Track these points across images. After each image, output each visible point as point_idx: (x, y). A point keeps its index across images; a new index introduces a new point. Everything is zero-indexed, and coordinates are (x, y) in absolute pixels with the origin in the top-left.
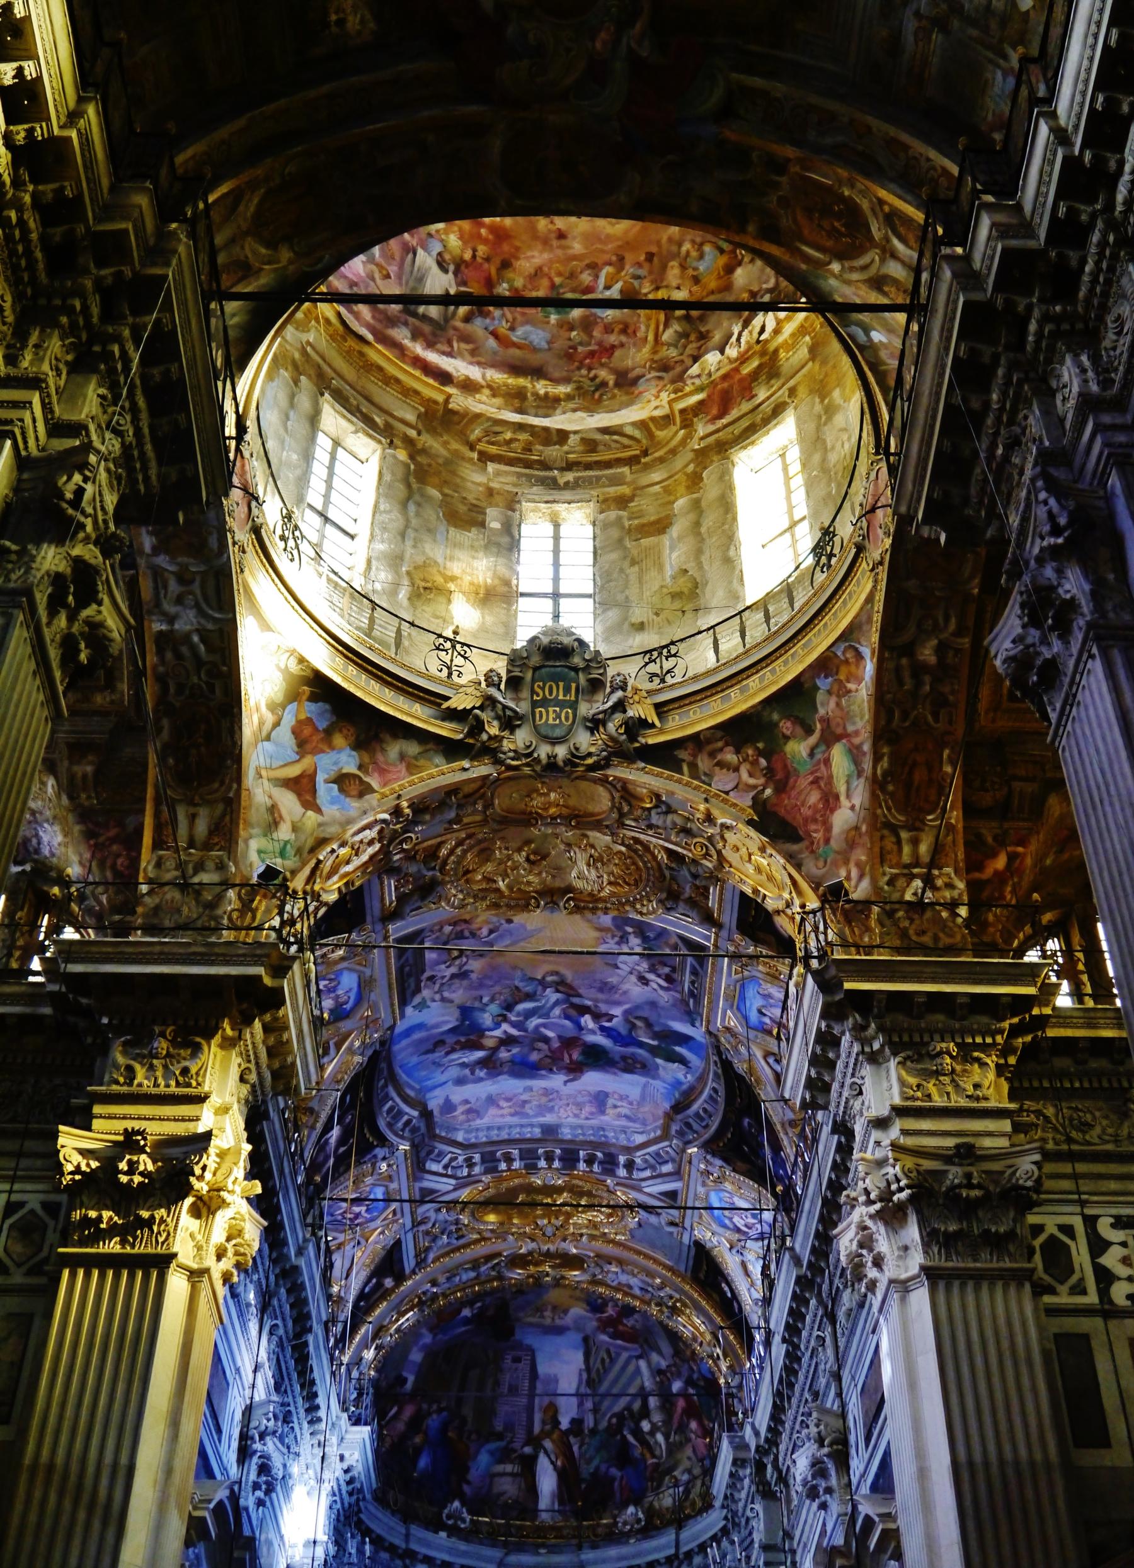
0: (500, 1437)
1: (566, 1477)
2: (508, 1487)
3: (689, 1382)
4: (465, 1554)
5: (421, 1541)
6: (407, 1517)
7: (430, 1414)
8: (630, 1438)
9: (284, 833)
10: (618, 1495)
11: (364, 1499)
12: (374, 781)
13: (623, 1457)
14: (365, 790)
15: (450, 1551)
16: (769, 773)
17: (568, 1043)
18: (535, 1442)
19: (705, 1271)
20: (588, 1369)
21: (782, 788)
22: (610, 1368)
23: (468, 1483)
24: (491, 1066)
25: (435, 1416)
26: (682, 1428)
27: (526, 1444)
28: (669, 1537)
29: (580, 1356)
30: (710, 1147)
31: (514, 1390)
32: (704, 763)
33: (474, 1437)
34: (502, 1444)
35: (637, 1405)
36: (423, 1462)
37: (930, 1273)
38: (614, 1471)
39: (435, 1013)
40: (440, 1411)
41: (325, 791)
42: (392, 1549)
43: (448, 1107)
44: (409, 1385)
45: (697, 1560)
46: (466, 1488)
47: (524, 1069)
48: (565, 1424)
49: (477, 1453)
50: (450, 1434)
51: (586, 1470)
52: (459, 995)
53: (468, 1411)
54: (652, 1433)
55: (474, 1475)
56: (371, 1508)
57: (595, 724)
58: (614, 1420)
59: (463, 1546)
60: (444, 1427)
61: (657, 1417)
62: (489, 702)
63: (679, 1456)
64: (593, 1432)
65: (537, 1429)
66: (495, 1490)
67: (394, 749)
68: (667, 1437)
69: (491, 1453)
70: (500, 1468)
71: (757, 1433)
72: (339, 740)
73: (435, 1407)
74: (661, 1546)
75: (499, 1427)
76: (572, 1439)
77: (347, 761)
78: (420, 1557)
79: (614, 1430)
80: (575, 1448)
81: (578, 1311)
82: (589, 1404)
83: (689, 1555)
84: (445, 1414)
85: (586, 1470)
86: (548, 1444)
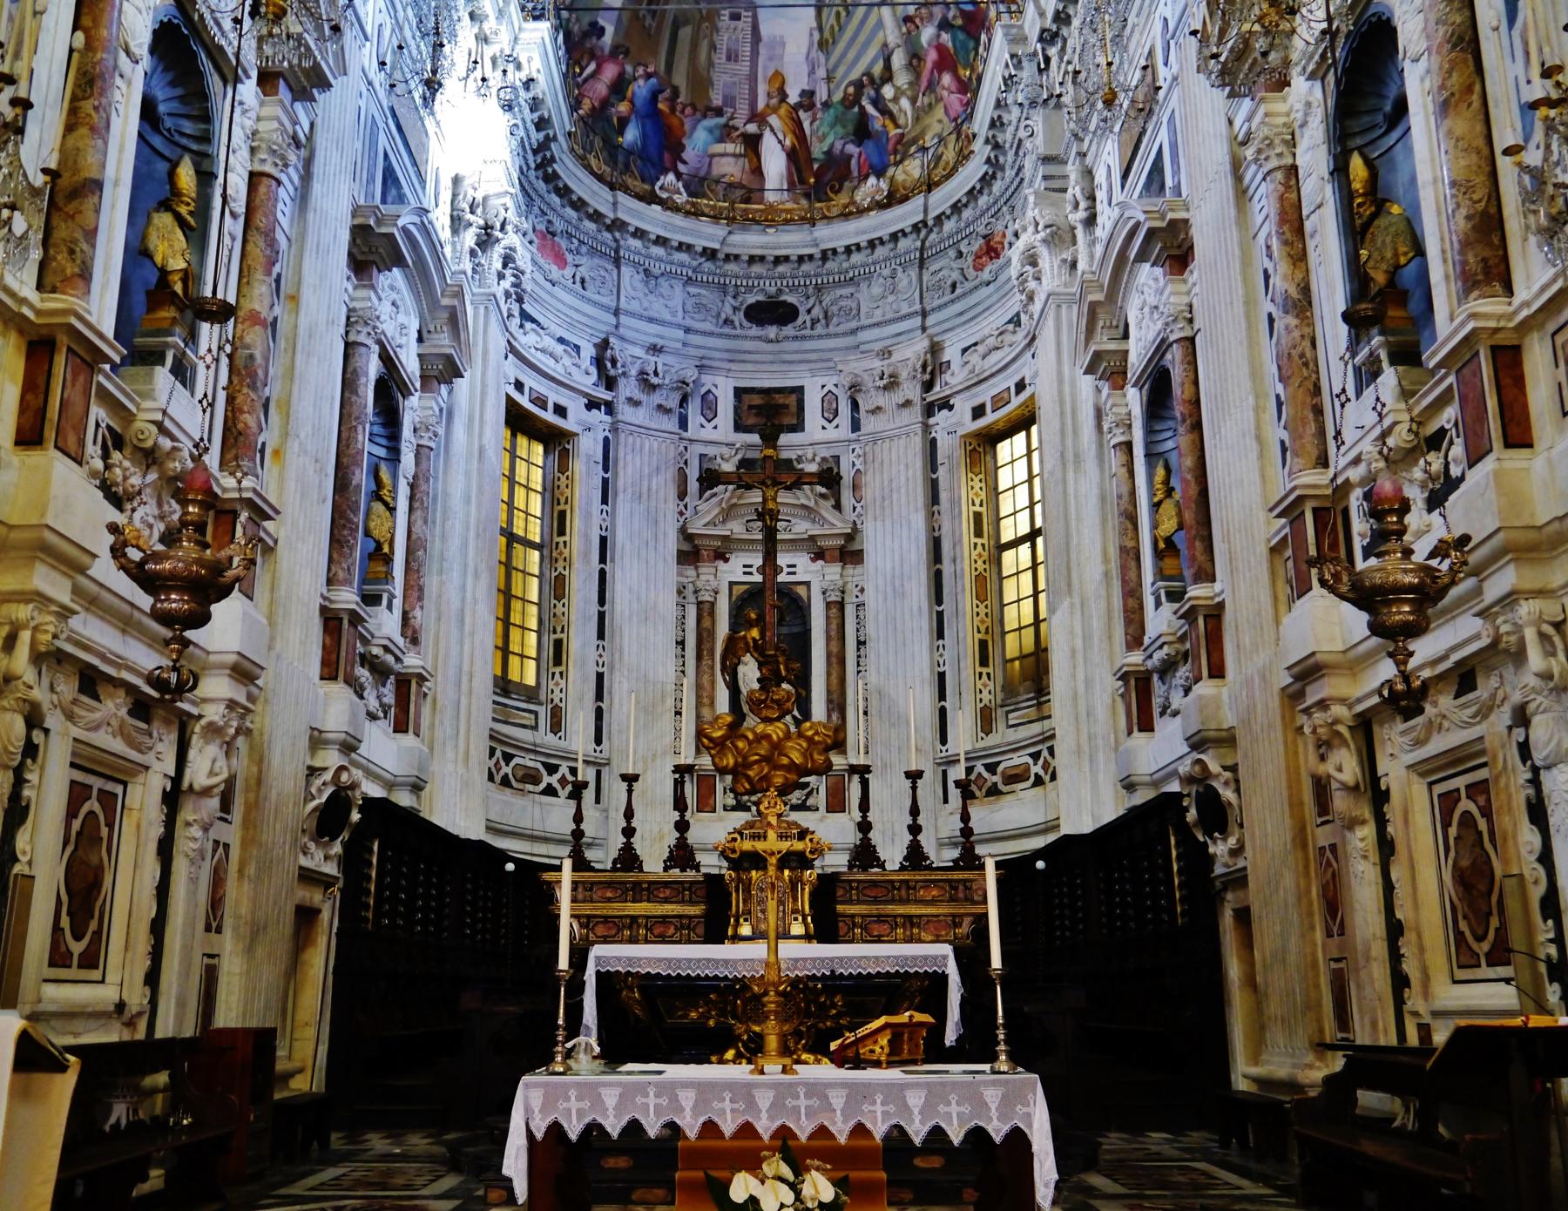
0: (719, 112)
1: (797, 157)
2: (730, 168)
3: (945, 25)
4: (682, 230)
5: (630, 211)
7: (635, 79)
8: (870, 109)
10: (855, 174)
11: (555, 138)
13: (862, 131)
15: (665, 226)
18: (757, 117)
20: (820, 29)
22: (847, 23)
23: (685, 162)
25: (641, 82)
26: (931, 87)
27: (750, 121)
28: (918, 201)
31: (732, 56)
33: (688, 110)
34: (722, 120)
35: (877, 70)
36: (631, 135)
38: (852, 149)
40: (648, 76)
42: (596, 217)
44: (608, 38)
45: (949, 226)
46: (681, 168)
48: (793, 98)
49: (694, 128)
50: (660, 106)
51: (818, 150)
53: (680, 79)
54: (896, 100)
56: (564, 157)
58: (851, 90)
59: (678, 220)
60: (654, 96)
61: (902, 79)
63: (927, 121)
64: (826, 105)
65: (761, 105)
66: (716, 172)
68: (913, 101)
69: (710, 130)
70: (719, 148)
71: (1042, 14)
73: (641, 71)
74: (904, 215)
75: (717, 101)
76: (801, 113)
78: (632, 229)
79: (851, 101)
80: (806, 125)
82: (821, 73)
83: (939, 220)
84: (653, 80)
85: (818, 150)
86: (773, 120)
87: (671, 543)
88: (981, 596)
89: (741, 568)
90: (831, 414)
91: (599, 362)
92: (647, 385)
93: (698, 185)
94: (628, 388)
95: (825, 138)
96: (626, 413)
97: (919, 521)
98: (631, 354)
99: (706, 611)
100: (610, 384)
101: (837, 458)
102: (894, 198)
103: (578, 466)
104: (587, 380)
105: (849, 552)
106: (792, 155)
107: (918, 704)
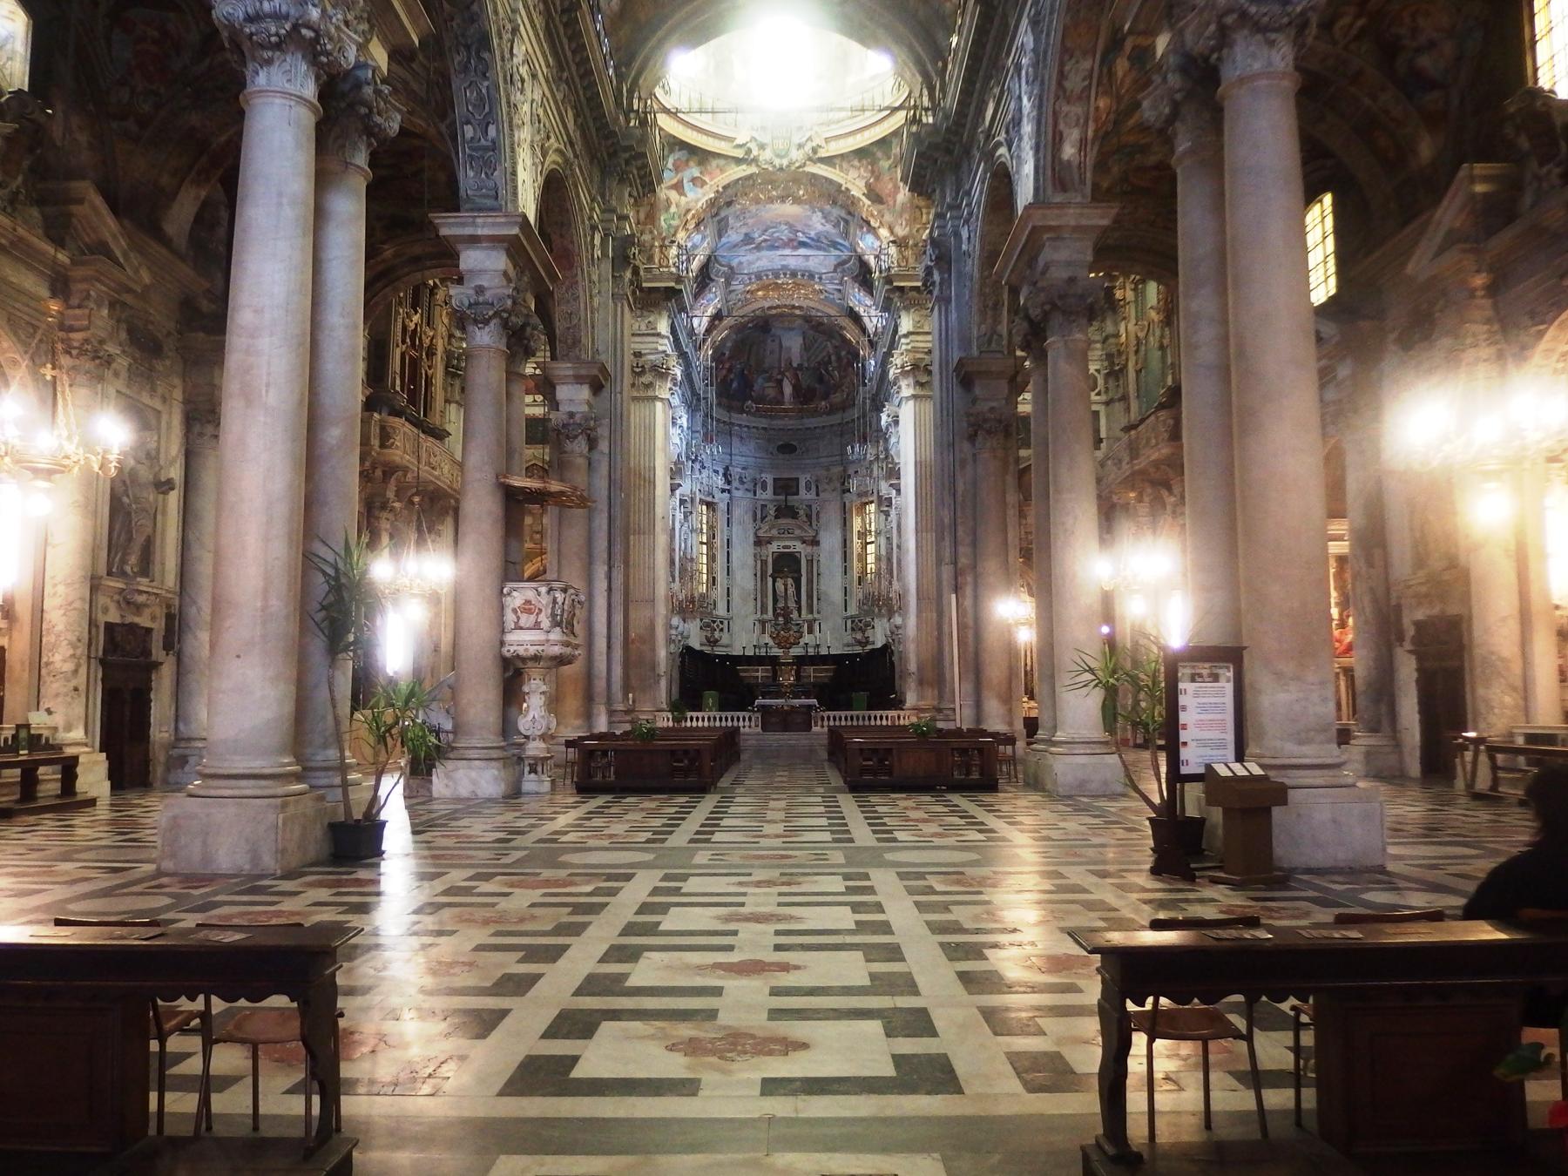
1: (796, 388)
2: (771, 392)
6: (729, 409)
9: (673, 209)
12: (706, 179)
13: (821, 380)
14: (704, 183)
16: (873, 172)
17: (791, 240)
18: (782, 374)
19: (856, 318)
21: (877, 178)
24: (758, 248)
29: (800, 340)
30: (855, 279)
32: (845, 165)
36: (735, 385)
37: (915, 397)
39: (733, 236)
41: (687, 186)
43: (741, 263)
47: (773, 247)
51: (804, 385)
52: (744, 230)
55: (756, 387)
57: (800, 146)
62: (753, 139)
67: (714, 163)
72: (692, 163)
74: (836, 418)
77: (695, 171)
81: (799, 322)
85: (804, 385)
87: (752, 539)
88: (859, 561)
89: (774, 547)
90: (808, 489)
91: (725, 475)
92: (742, 482)
93: (760, 400)
94: (735, 484)
95: (806, 380)
96: (736, 494)
97: (839, 533)
98: (736, 471)
99: (764, 563)
100: (729, 483)
101: (810, 507)
102: (832, 410)
103: (719, 514)
104: (720, 481)
105: (815, 542)
106: (794, 387)
107: (837, 596)
